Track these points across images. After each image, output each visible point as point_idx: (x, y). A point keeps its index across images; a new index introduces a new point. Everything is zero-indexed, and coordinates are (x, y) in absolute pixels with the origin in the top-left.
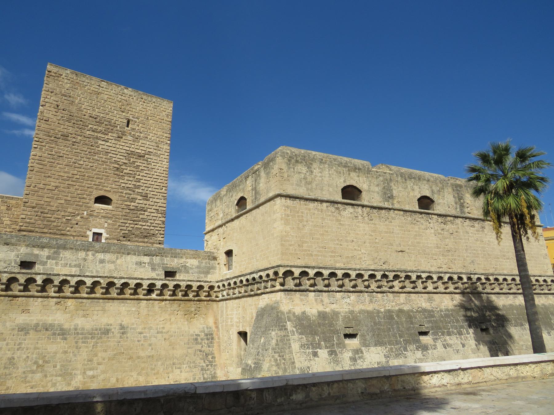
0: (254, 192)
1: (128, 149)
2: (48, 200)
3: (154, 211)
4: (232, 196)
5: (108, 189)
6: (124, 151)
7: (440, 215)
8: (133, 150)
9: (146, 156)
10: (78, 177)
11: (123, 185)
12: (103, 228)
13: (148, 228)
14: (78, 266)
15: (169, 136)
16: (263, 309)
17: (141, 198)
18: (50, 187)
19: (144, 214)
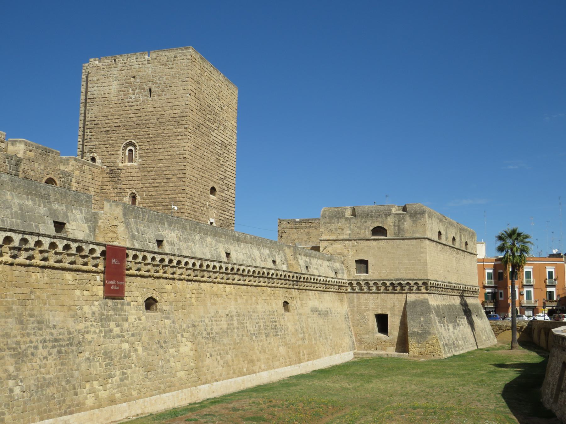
0: (397, 228)
1: (222, 139)
2: (194, 191)
3: (231, 201)
4: (366, 222)
5: (215, 180)
6: (220, 142)
7: (457, 249)
8: (223, 140)
9: (229, 147)
10: (204, 168)
11: (220, 176)
12: (213, 218)
13: (228, 217)
14: (317, 269)
15: (235, 124)
16: (413, 302)
17: (226, 189)
18: (195, 179)
19: (227, 205)
